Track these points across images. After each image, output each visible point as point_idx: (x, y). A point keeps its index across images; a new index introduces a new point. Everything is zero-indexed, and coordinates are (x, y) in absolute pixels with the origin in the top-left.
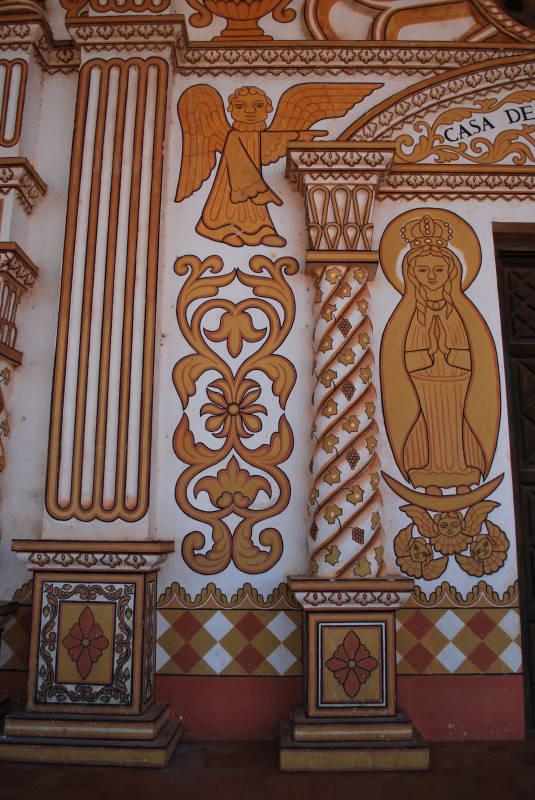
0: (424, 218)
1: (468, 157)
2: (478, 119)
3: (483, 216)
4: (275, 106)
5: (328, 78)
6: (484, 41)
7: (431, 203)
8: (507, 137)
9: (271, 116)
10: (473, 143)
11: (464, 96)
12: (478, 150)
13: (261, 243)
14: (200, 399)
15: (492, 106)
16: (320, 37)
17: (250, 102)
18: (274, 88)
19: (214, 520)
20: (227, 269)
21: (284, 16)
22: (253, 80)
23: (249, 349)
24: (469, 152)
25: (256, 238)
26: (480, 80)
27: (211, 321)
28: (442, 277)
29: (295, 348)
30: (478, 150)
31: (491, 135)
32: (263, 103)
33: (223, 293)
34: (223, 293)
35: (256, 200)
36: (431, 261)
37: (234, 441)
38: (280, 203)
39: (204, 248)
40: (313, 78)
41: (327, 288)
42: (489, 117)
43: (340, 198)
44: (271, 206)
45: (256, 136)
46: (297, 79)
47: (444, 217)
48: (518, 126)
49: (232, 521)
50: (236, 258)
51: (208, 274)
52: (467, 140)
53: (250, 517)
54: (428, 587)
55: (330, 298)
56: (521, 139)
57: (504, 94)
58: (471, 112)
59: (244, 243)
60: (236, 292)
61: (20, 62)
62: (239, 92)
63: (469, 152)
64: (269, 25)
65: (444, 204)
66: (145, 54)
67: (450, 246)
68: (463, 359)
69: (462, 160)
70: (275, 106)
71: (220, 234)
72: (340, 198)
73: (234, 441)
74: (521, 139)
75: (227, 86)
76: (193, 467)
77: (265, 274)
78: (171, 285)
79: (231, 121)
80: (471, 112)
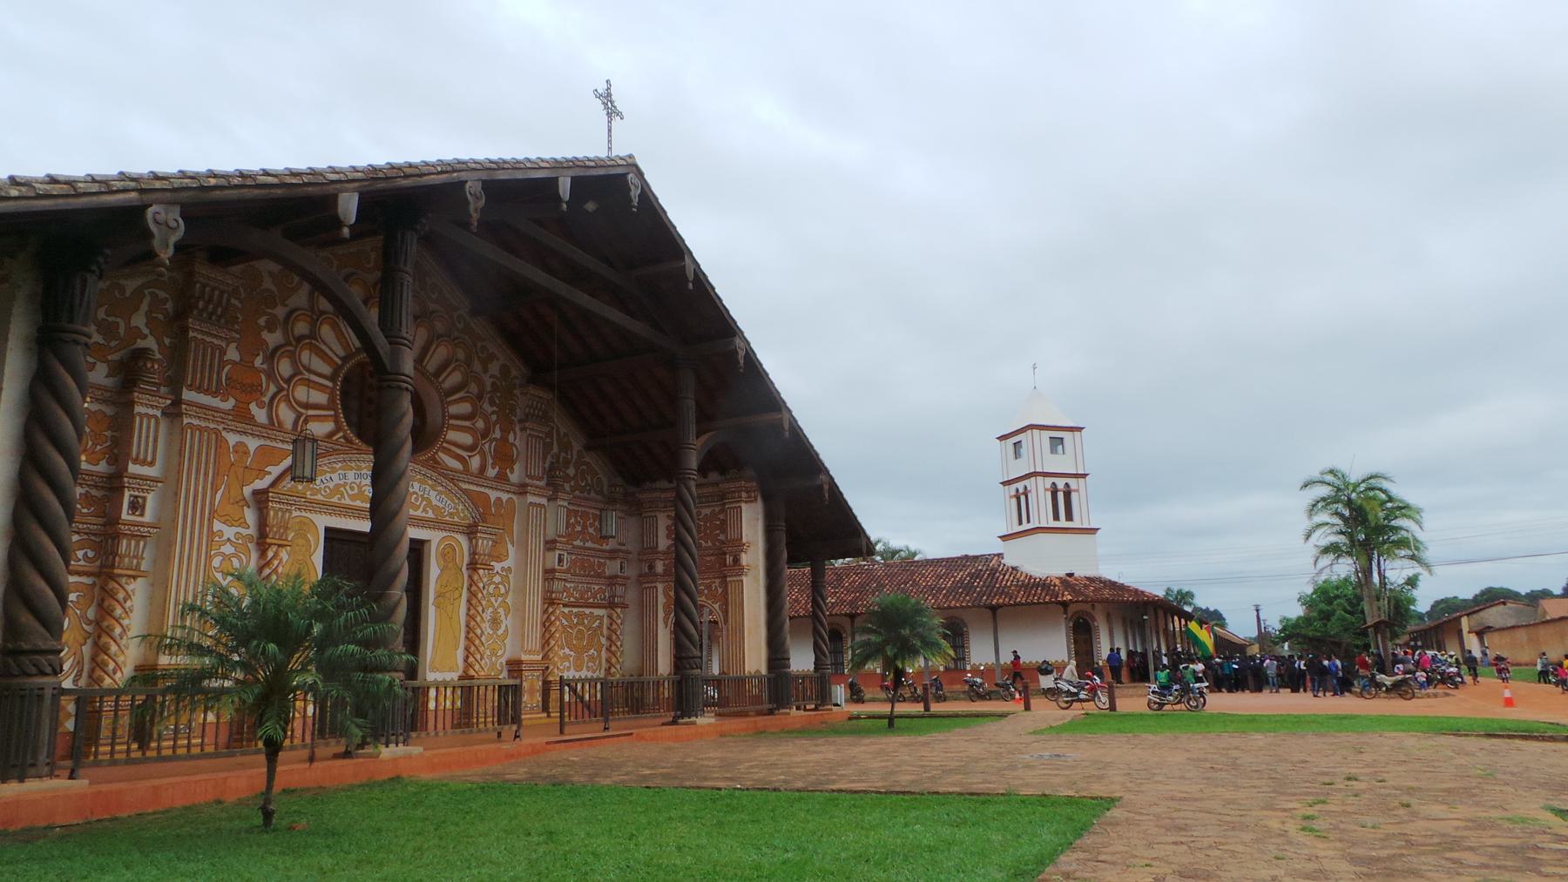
0: (301, 522)
1: (322, 495)
2: (328, 476)
3: (323, 521)
4: (252, 453)
5: (274, 444)
6: (337, 440)
7: (304, 514)
8: (337, 486)
9: (250, 459)
10: (325, 487)
11: (325, 464)
12: (326, 492)
13: (239, 526)
15: (334, 471)
16: (276, 425)
17: (241, 449)
18: (253, 444)
20: (225, 538)
21: (260, 406)
22: (244, 439)
24: (323, 492)
25: (237, 524)
26: (332, 459)
28: (304, 549)
30: (326, 492)
31: (331, 485)
32: (246, 453)
33: (223, 549)
34: (223, 549)
35: (240, 504)
36: (301, 542)
38: (249, 507)
40: (268, 442)
41: (270, 554)
42: (332, 476)
43: (280, 514)
44: (245, 508)
45: (242, 469)
46: (262, 442)
47: (307, 521)
48: (342, 482)
51: (217, 539)
52: (323, 486)
55: (271, 559)
56: (342, 489)
57: (340, 465)
58: (326, 472)
59: (232, 525)
60: (228, 549)
61: (155, 417)
62: (237, 443)
63: (323, 492)
64: (253, 407)
65: (308, 515)
66: (212, 426)
67: (308, 535)
69: (319, 497)
70: (252, 453)
71: (223, 519)
72: (280, 514)
74: (342, 489)
75: (232, 439)
77: (240, 541)
79: (233, 459)
80: (326, 472)
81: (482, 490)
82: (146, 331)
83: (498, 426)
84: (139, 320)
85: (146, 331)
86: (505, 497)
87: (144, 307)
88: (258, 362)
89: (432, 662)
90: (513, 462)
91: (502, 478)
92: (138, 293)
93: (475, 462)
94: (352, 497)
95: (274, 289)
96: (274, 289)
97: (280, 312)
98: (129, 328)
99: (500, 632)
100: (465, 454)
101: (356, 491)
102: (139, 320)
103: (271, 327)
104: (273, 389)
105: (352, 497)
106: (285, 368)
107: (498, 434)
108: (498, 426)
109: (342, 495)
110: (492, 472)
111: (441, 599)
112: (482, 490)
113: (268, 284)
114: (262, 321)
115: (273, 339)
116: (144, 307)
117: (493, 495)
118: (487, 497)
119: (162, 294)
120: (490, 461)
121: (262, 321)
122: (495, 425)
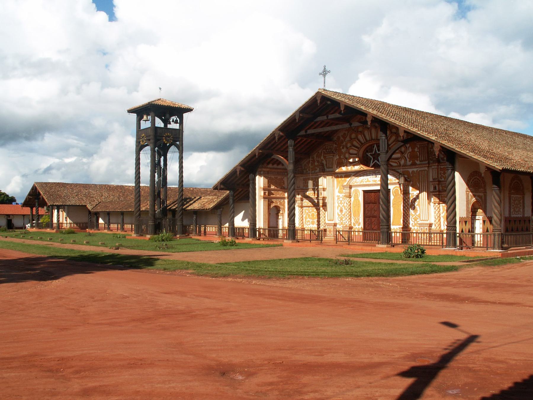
3: (361, 189)
14: (339, 210)
19: (340, 221)
23: (342, 205)
27: (339, 202)
29: (345, 204)
37: (341, 213)
39: (339, 194)
49: (342, 221)
50: (341, 195)
53: (343, 221)
54: (355, 227)
60: (341, 199)
68: (358, 205)
73: (341, 213)
76: (339, 216)
78: (336, 198)
81: (407, 170)
82: (323, 159)
83: (410, 148)
84: (322, 158)
85: (323, 159)
86: (415, 170)
87: (323, 155)
88: (342, 157)
89: (392, 223)
90: (417, 157)
91: (414, 164)
92: (321, 152)
93: (402, 162)
94: (366, 182)
95: (343, 139)
96: (343, 139)
97: (344, 144)
98: (321, 160)
99: (417, 214)
100: (396, 161)
101: (367, 180)
102: (322, 158)
103: (343, 148)
104: (345, 161)
105: (366, 182)
106: (347, 156)
107: (410, 150)
108: (410, 148)
109: (363, 182)
110: (409, 163)
111: (395, 205)
112: (407, 170)
113: (342, 138)
114: (341, 148)
115: (344, 150)
116: (323, 155)
117: (410, 170)
118: (408, 171)
119: (324, 151)
120: (408, 160)
121: (341, 148)
122: (409, 147)
